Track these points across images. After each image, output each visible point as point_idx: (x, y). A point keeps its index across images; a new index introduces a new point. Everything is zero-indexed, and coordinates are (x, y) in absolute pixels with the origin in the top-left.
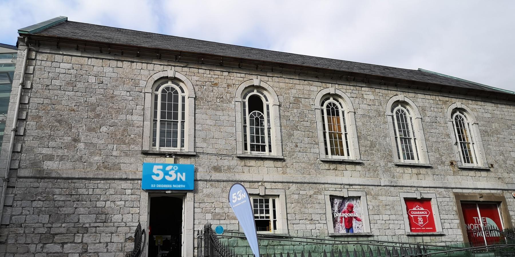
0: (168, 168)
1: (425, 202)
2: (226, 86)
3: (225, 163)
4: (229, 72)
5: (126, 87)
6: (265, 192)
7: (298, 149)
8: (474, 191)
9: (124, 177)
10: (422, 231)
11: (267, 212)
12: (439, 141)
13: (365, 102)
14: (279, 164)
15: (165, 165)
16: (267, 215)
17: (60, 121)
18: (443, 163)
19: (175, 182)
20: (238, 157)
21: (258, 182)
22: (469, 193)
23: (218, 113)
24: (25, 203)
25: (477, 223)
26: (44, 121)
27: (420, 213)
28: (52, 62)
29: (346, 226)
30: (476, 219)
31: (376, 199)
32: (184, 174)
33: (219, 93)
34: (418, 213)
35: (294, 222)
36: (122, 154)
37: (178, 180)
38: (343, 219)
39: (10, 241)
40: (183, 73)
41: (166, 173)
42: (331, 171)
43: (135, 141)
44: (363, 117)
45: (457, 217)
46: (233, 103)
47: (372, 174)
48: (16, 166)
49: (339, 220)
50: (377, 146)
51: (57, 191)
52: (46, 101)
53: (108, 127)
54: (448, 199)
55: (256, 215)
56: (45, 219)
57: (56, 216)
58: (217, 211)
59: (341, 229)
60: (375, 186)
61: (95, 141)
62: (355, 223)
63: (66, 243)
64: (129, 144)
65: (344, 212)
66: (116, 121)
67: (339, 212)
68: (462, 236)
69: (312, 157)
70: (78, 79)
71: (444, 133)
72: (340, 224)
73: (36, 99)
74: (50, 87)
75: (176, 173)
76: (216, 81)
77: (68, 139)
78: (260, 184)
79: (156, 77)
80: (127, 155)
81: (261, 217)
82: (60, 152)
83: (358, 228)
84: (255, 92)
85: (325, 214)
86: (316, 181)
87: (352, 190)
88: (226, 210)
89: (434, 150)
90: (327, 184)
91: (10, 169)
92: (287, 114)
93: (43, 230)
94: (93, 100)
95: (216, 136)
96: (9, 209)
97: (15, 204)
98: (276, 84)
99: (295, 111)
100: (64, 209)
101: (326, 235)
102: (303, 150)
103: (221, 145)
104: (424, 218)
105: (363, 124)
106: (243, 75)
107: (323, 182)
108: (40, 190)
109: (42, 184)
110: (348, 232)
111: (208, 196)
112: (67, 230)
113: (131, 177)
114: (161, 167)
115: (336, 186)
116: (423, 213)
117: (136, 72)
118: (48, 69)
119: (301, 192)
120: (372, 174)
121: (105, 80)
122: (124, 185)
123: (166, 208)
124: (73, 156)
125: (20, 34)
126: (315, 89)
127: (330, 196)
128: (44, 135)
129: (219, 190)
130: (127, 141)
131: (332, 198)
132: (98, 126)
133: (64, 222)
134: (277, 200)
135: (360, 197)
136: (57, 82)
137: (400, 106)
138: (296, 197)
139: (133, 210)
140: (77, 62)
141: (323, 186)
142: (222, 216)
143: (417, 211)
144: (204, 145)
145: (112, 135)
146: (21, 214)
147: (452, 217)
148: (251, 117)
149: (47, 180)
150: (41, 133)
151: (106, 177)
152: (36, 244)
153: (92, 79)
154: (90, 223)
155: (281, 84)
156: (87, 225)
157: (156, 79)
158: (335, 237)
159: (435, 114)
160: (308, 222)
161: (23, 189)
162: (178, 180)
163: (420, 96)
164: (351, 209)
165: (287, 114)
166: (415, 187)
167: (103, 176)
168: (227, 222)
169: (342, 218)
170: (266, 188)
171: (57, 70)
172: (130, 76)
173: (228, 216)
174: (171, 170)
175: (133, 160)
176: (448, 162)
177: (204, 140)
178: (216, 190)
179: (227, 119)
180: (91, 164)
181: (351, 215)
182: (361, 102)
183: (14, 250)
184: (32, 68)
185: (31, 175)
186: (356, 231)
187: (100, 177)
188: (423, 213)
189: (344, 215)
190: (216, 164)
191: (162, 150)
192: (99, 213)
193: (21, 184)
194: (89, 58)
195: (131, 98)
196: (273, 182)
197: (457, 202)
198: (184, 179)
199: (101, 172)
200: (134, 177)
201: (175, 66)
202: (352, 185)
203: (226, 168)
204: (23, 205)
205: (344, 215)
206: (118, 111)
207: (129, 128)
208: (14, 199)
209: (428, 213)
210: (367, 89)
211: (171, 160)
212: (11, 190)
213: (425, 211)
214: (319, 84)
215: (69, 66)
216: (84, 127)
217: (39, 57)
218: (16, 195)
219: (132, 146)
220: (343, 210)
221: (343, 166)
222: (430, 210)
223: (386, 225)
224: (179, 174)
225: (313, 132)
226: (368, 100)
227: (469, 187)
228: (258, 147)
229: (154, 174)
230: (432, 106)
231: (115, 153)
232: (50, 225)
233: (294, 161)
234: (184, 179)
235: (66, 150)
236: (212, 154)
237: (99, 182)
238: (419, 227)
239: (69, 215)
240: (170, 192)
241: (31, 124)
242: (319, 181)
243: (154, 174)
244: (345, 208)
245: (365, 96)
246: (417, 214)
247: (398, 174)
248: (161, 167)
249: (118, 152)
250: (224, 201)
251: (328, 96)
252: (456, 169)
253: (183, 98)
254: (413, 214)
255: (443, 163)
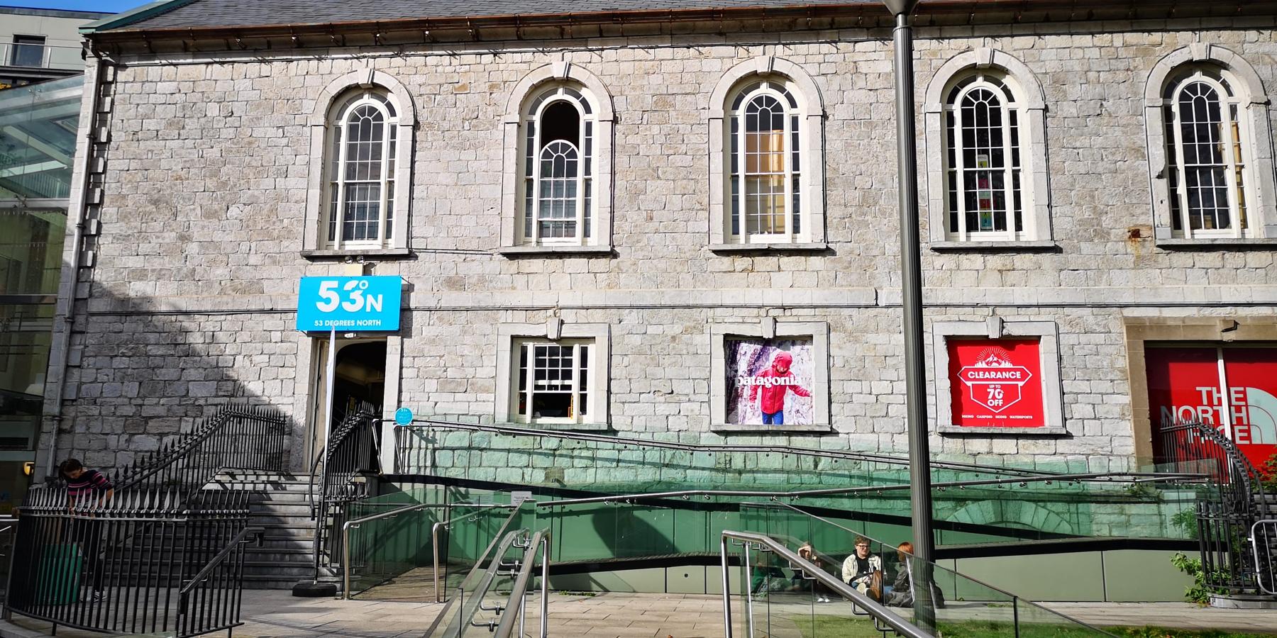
0: (348, 286)
1: (1020, 347)
2: (485, 87)
3: (474, 268)
4: (495, 55)
5: (277, 118)
6: (560, 331)
7: (652, 226)
8: (1207, 311)
9: (268, 307)
10: (999, 423)
11: (567, 375)
12: (1100, 170)
13: (861, 83)
14: (602, 263)
15: (343, 280)
16: (567, 382)
17: (155, 203)
18: (1103, 235)
19: (362, 314)
20: (505, 254)
21: (546, 309)
22: (1184, 319)
23: (468, 155)
24: (102, 361)
25: (1210, 404)
26: (130, 204)
27: (999, 375)
28: (143, 82)
29: (764, 407)
30: (1210, 394)
31: (857, 341)
32: (380, 297)
33: (471, 106)
34: (993, 375)
35: (627, 398)
36: (267, 261)
37: (368, 309)
38: (760, 391)
39: (79, 429)
40: (390, 71)
41: (345, 296)
42: (736, 275)
43: (290, 231)
44: (849, 126)
45: (1126, 387)
46: (501, 127)
47: (854, 277)
48: (84, 293)
49: (747, 393)
50: (882, 202)
51: (152, 338)
52: (133, 165)
53: (241, 206)
54: (1100, 338)
55: (541, 382)
56: (132, 389)
57: (150, 386)
58: (450, 373)
59: (749, 415)
60: (859, 307)
61: (218, 236)
62: (789, 400)
63: (167, 434)
64: (280, 239)
65: (765, 375)
66: (256, 193)
67: (750, 375)
68: (1131, 441)
69: (686, 242)
70: (188, 113)
71: (1125, 143)
72: (750, 404)
73: (116, 162)
74: (140, 135)
75: (364, 295)
76: (463, 81)
77: (170, 237)
78: (551, 312)
79: (334, 89)
80: (274, 262)
81: (550, 387)
82: (157, 263)
83: (795, 413)
84: (560, 95)
85: (709, 379)
86: (691, 303)
87: (791, 319)
88: (470, 372)
89: (1074, 199)
90: (722, 306)
91: (76, 300)
92: (632, 139)
93: (129, 411)
94: (214, 153)
95: (456, 210)
96: (76, 371)
97: (85, 364)
98: (612, 68)
99: (656, 129)
100: (163, 371)
101: (705, 427)
102: (665, 227)
103: (469, 230)
104: (1009, 391)
105: (847, 145)
106: (528, 56)
107: (709, 302)
108: (124, 337)
109: (129, 326)
110: (768, 418)
111: (432, 342)
112: (169, 410)
113: (279, 308)
114: (335, 284)
115: (745, 312)
116: (1007, 375)
117: (297, 82)
118: (135, 100)
119: (650, 330)
120: (854, 277)
121: (238, 109)
122: (270, 322)
123: (359, 368)
124: (179, 270)
125: (85, 36)
126: (716, 65)
127: (726, 336)
128: (130, 232)
129: (456, 329)
130: (275, 234)
131: (732, 343)
132: (224, 206)
133: (164, 396)
134: (592, 349)
135: (811, 337)
136: (150, 124)
137: (980, 79)
138: (636, 340)
139: (284, 373)
140: (186, 78)
141: (710, 312)
142: (459, 384)
143: (989, 370)
144: (429, 231)
145: (244, 224)
146: (95, 381)
147: (1106, 386)
148: (546, 155)
149: (135, 318)
150: (124, 229)
151: (236, 308)
152: (119, 435)
153: (213, 110)
154: (206, 398)
155: (624, 66)
156: (202, 402)
157: (334, 93)
158: (727, 434)
159: (1099, 89)
160: (662, 399)
161: (98, 336)
162: (368, 309)
163: (1051, 40)
164: (784, 366)
165: (632, 139)
166: (987, 306)
167: (230, 308)
168: (470, 396)
169: (755, 388)
170: (562, 322)
171: (153, 99)
172: (284, 93)
173: (472, 384)
174: (353, 290)
175: (286, 271)
176: (1122, 231)
177: (431, 219)
178: (451, 328)
179: (484, 168)
180: (209, 284)
181: (781, 381)
182: (847, 85)
183: (84, 444)
184: (108, 100)
185: (109, 309)
186: (790, 421)
187: (225, 308)
188: (1007, 375)
189: (761, 381)
190: (452, 274)
191: (347, 248)
192: (222, 379)
193: (96, 327)
194: (208, 64)
195: (285, 141)
196: (583, 308)
197: (1131, 346)
198: (379, 308)
199: (225, 298)
200: (286, 307)
201: (374, 57)
202: (791, 308)
203: (474, 280)
204: (98, 365)
205: (761, 381)
206: (261, 171)
207: (281, 206)
208: (83, 353)
209: (1024, 375)
210: (872, 45)
211: (357, 268)
212: (78, 338)
213: (1015, 370)
214: (729, 50)
215: (172, 87)
216: (198, 211)
217: (121, 76)
218: (86, 346)
219: (285, 243)
220: (763, 370)
221: (773, 260)
222: (1034, 366)
223: (878, 406)
224: (370, 297)
225: (697, 181)
226: (870, 78)
227: (1188, 301)
228: (557, 225)
229: (321, 299)
230: (1095, 67)
231: (253, 260)
232: (139, 401)
233: (640, 254)
234: (379, 308)
235: (167, 259)
236: (445, 251)
237: (223, 317)
238: (988, 412)
239: (170, 382)
240: (351, 335)
241: (108, 211)
242: (699, 302)
243: (321, 299)
244: (768, 364)
245: (863, 68)
246: (987, 379)
247: (937, 274)
248: (335, 284)
249: (259, 257)
250: (466, 352)
251: (753, 81)
252: (1150, 248)
253: (394, 128)
254: (975, 379)
255: (1103, 235)
